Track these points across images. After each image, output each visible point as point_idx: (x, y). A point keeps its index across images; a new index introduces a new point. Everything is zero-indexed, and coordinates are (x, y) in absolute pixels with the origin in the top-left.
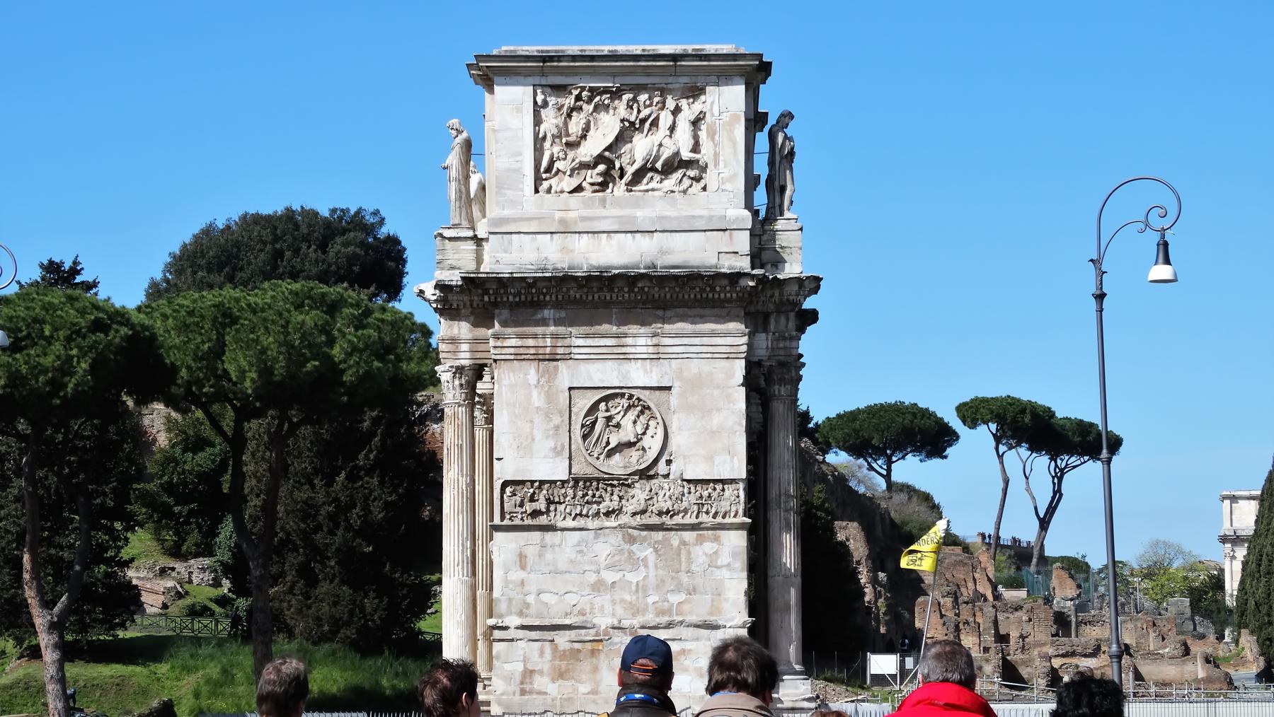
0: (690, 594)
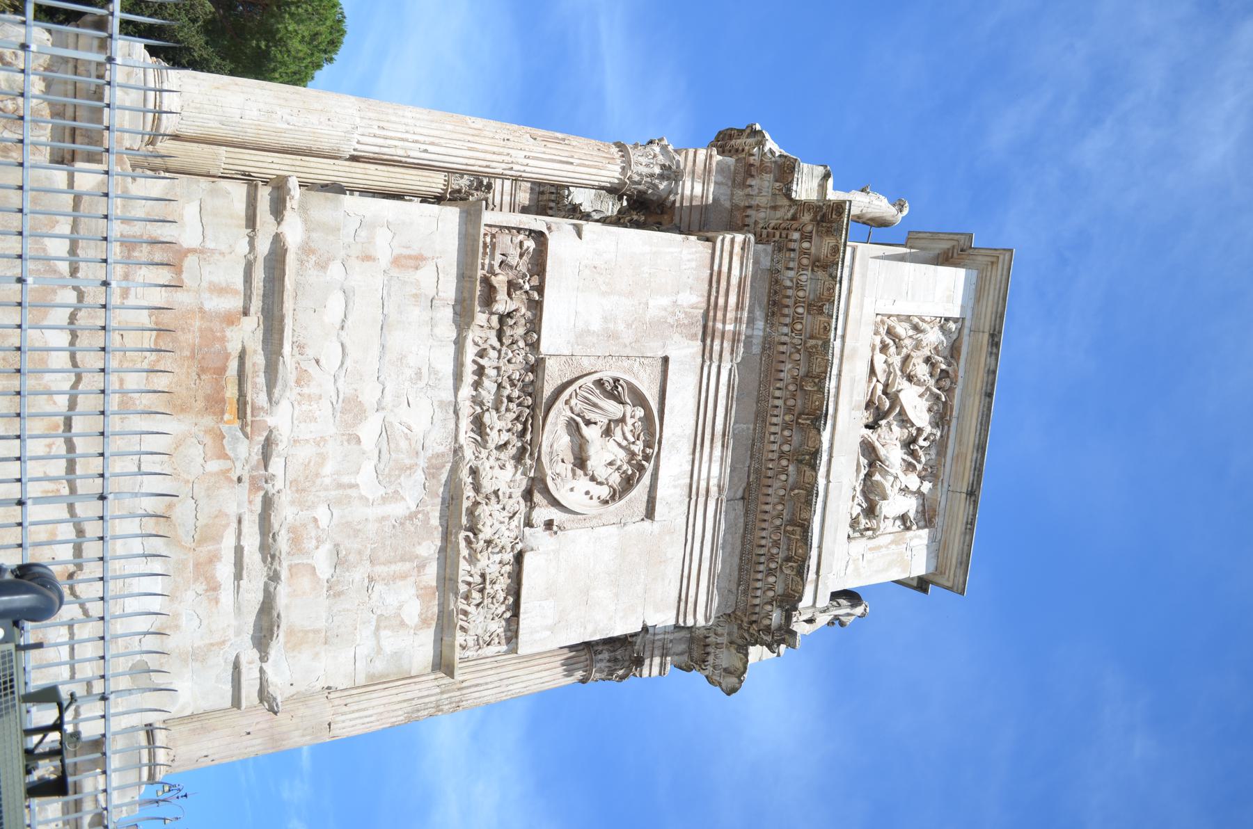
0: (330, 588)
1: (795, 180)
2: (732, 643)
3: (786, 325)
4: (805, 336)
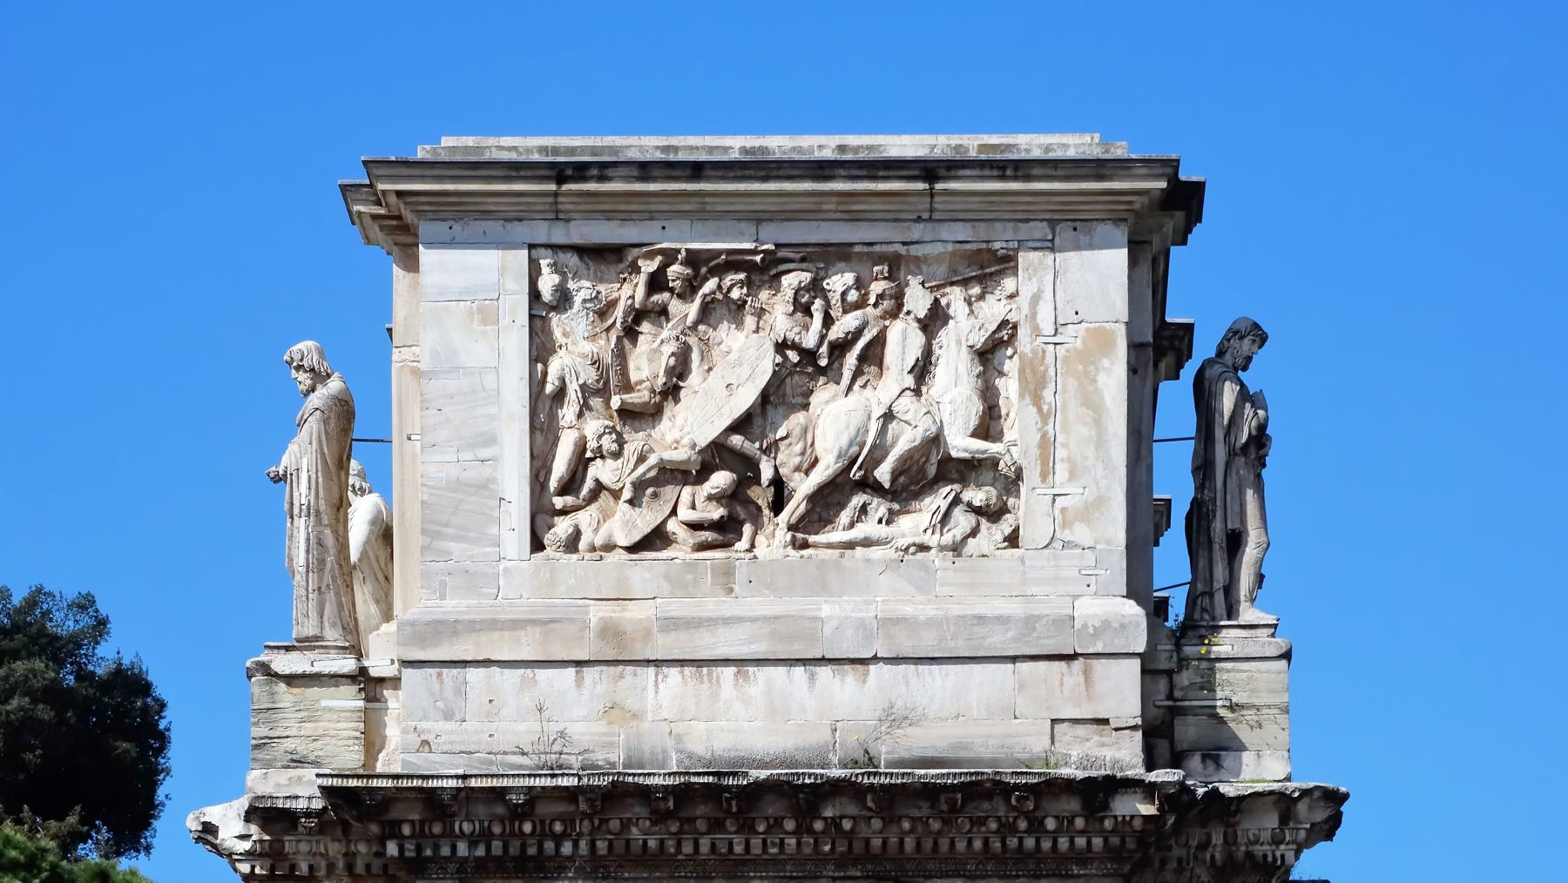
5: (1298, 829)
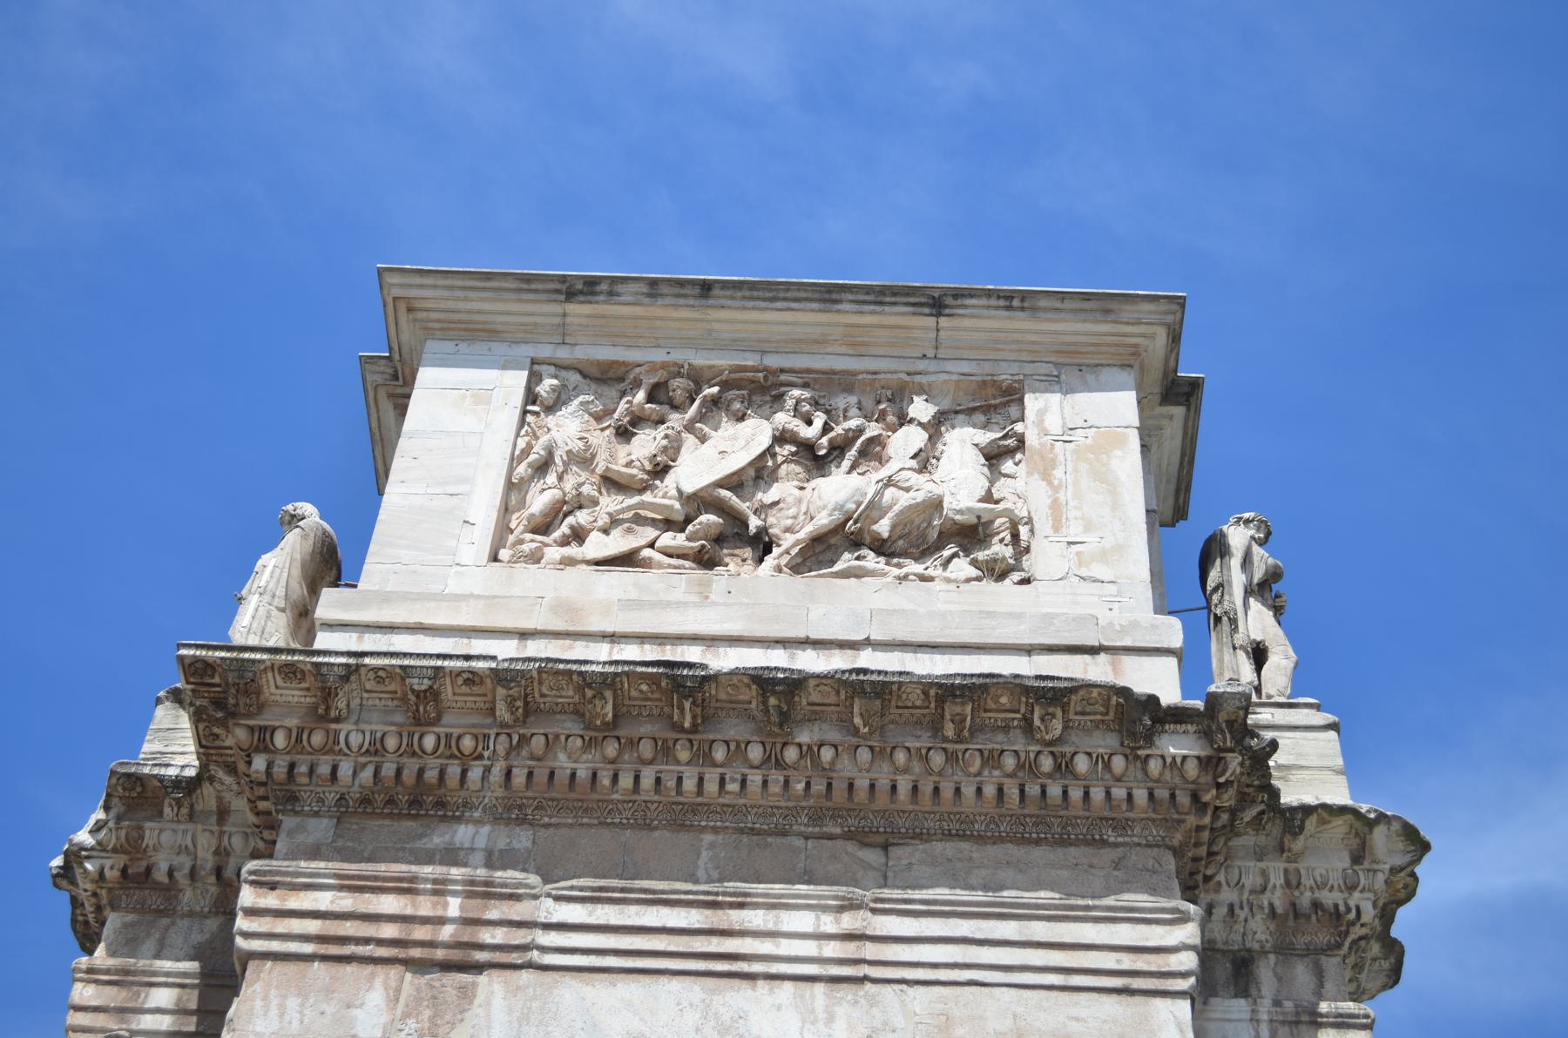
1: (156, 771)
2: (1281, 849)
3: (464, 773)
4: (489, 726)
5: (1375, 871)
